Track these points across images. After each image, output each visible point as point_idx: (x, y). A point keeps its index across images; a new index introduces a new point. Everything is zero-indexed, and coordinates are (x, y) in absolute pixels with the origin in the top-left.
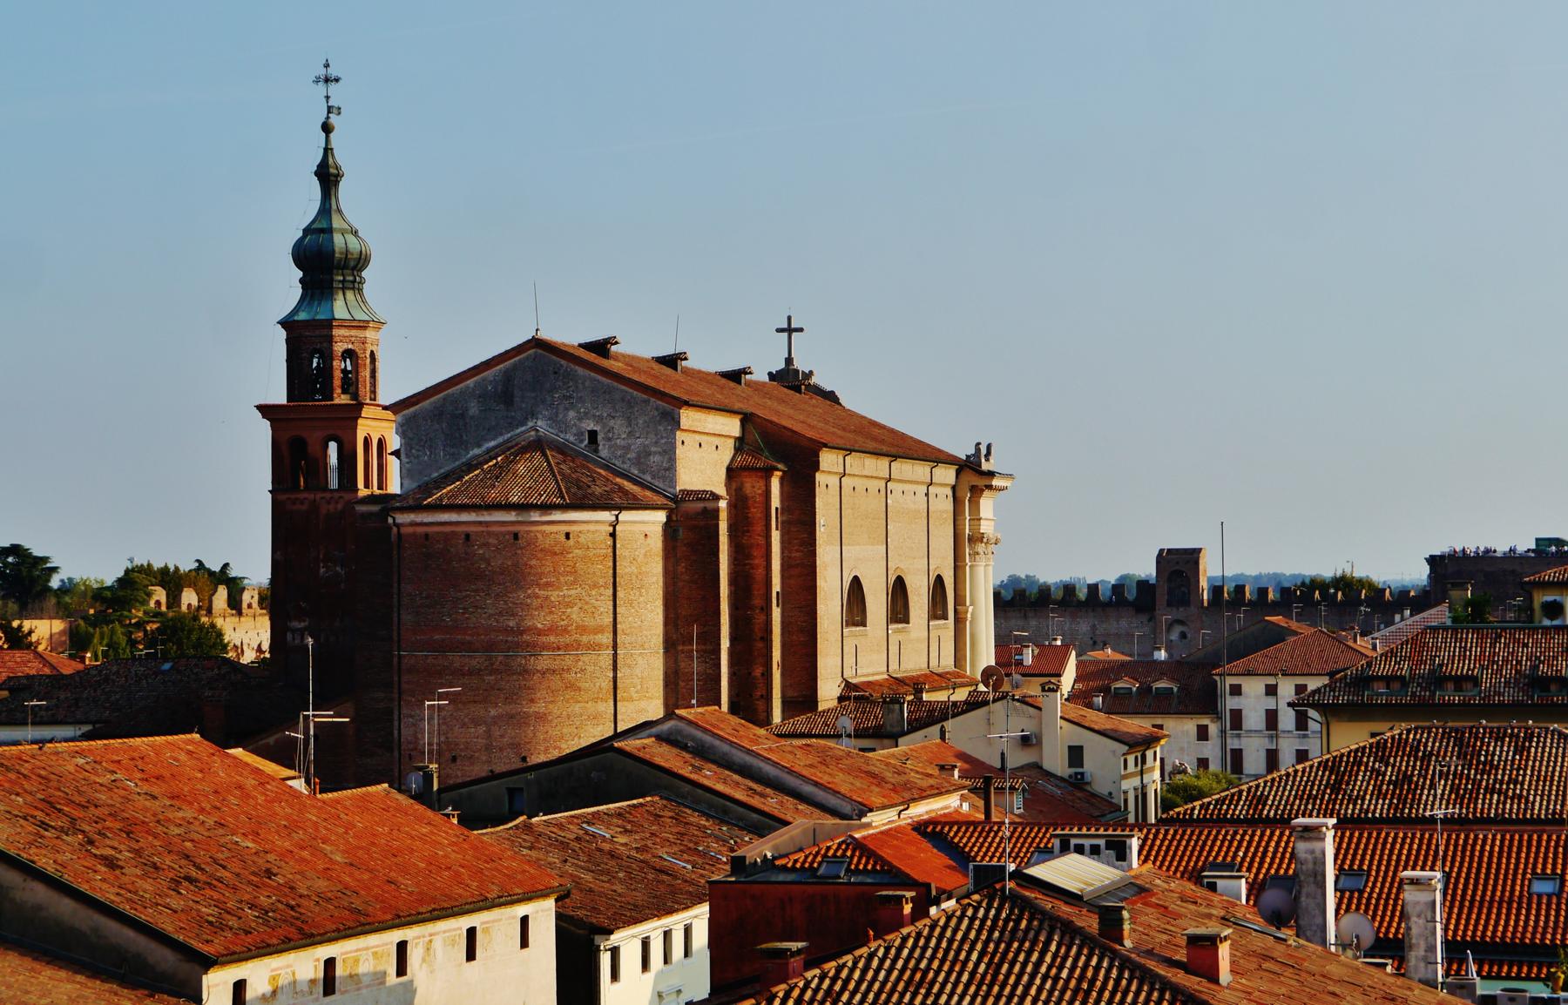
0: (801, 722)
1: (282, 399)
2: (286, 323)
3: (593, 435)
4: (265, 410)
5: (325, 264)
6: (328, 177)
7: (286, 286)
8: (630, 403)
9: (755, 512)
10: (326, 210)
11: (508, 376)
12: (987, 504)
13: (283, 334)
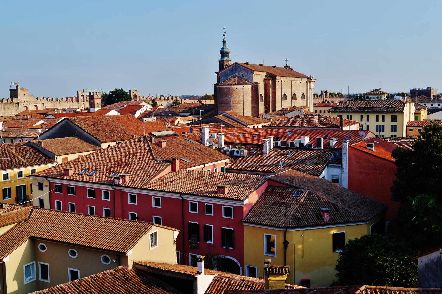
0: (274, 113)
6: (224, 42)
7: (219, 56)
8: (247, 71)
9: (268, 85)
10: (224, 46)
11: (232, 68)
12: (312, 84)
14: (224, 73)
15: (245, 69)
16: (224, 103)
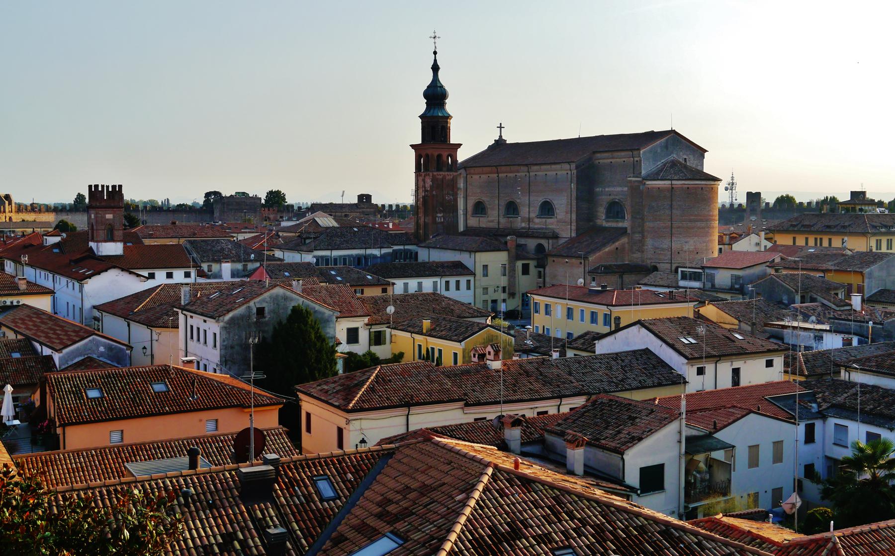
1: (419, 141)
5: (435, 96)
6: (435, 68)
7: (421, 106)
11: (667, 140)
14: (651, 151)
16: (702, 221)
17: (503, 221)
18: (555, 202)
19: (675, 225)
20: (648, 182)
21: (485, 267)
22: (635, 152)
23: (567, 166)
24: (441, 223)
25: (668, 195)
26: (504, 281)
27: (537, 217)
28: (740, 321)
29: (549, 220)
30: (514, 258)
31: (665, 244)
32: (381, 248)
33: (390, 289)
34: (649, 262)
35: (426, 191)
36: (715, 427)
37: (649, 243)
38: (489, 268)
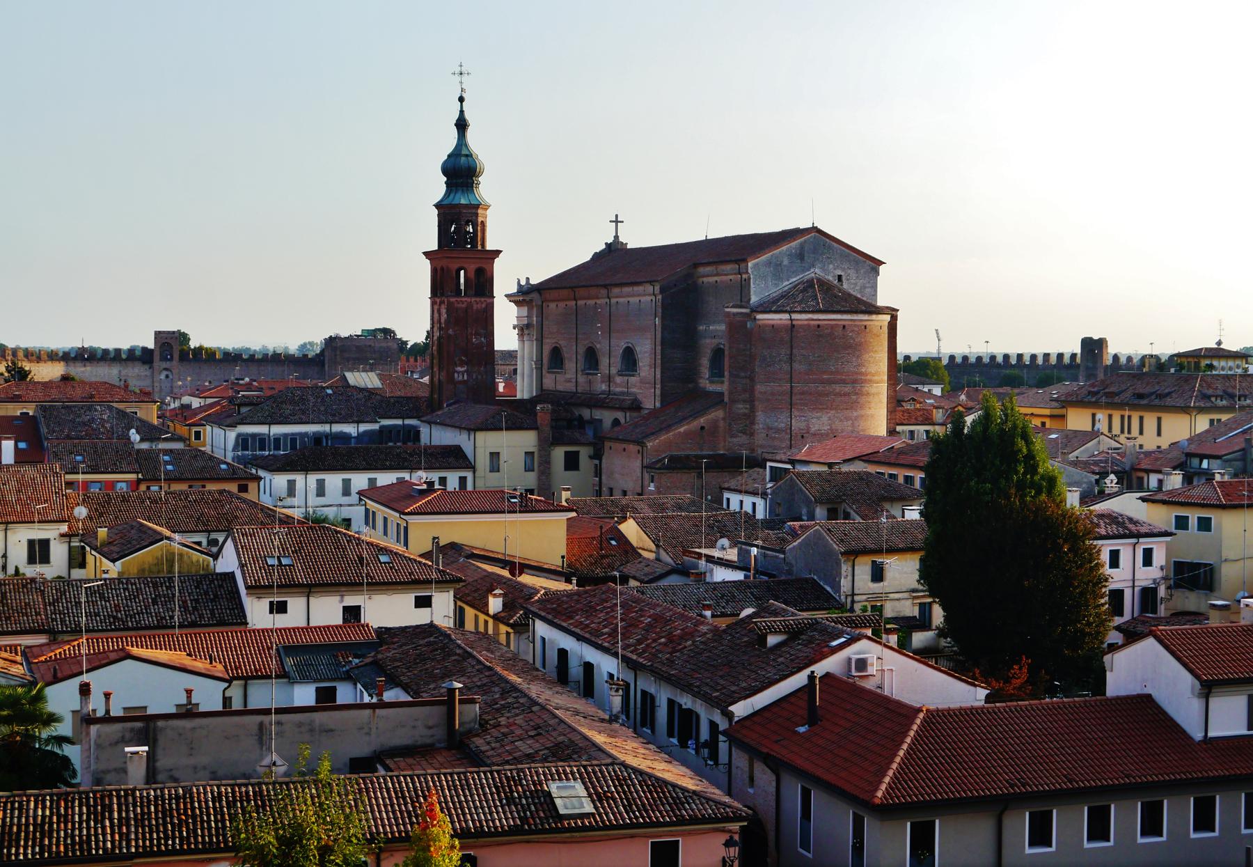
1: (433, 245)
2: (438, 206)
3: (840, 277)
4: (427, 254)
5: (461, 172)
6: (462, 125)
7: (438, 187)
8: (857, 262)
11: (802, 246)
13: (436, 212)
14: (768, 263)
15: (847, 256)
16: (844, 382)
17: (581, 379)
18: (638, 349)
19: (795, 391)
20: (759, 316)
21: (495, 456)
22: (743, 265)
23: (650, 288)
24: (464, 382)
25: (787, 338)
26: (531, 480)
27: (620, 374)
28: (657, 546)
29: (632, 379)
30: (546, 444)
31: (781, 421)
32: (358, 422)
33: (252, 486)
34: (759, 451)
35: (440, 329)
36: (55, 676)
37: (760, 417)
38: (503, 458)
